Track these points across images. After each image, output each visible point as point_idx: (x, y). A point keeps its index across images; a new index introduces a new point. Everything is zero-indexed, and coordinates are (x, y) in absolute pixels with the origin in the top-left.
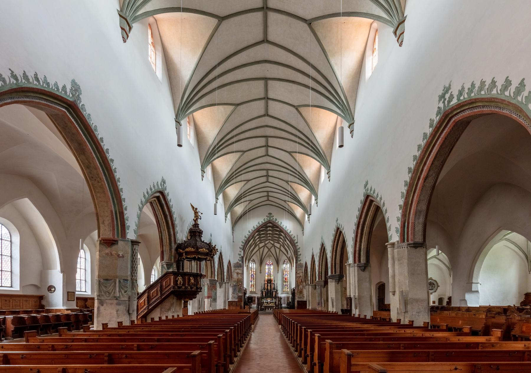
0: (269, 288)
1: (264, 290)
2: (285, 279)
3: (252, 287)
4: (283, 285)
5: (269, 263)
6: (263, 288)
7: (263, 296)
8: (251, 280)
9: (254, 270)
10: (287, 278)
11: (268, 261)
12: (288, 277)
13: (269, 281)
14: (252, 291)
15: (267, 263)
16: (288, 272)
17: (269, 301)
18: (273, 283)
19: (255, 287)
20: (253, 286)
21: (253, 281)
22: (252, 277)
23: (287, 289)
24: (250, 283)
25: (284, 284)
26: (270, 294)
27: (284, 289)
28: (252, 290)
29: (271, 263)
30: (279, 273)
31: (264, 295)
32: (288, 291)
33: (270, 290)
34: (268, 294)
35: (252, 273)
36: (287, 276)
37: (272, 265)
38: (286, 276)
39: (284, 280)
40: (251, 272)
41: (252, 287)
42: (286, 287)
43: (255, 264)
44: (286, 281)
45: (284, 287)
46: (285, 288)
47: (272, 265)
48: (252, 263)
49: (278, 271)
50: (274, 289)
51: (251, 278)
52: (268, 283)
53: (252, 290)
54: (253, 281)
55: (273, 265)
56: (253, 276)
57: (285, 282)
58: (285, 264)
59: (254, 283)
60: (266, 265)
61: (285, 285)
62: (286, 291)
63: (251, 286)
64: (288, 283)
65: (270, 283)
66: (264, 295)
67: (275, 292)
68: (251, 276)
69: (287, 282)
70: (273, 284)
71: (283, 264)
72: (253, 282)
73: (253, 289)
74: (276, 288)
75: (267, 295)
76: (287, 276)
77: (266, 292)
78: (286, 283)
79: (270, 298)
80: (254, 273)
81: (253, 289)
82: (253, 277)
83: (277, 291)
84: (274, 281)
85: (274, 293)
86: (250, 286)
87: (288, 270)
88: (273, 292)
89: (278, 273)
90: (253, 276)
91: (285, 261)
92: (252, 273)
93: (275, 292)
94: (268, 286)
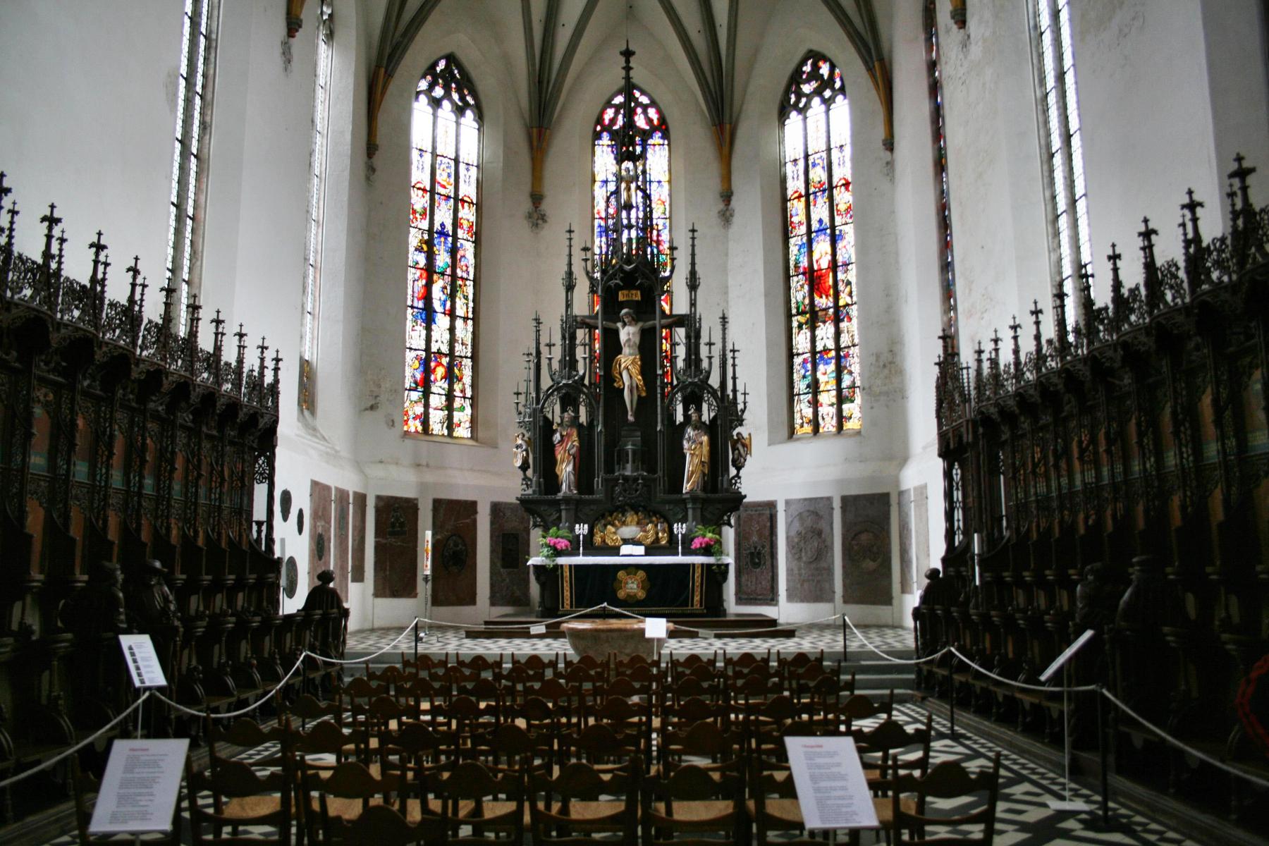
0: (628, 361)
1: (569, 401)
2: (814, 280)
3: (439, 386)
4: (791, 355)
5: (630, 115)
6: (546, 383)
7: (549, 479)
8: (427, 298)
9: (468, 190)
10: (834, 266)
11: (619, 99)
12: (847, 250)
13: (629, 281)
14: (437, 426)
15: (610, 113)
16: (843, 198)
17: (633, 554)
18: (681, 308)
19: (474, 386)
20: (450, 376)
21: (452, 314)
22: (443, 259)
23: (841, 399)
24: (415, 337)
25: (802, 341)
26: (646, 458)
27: (803, 409)
28: (437, 417)
29: (652, 113)
30: (737, 220)
31: (565, 470)
32: (848, 425)
33: (645, 404)
34: (614, 457)
35: (443, 216)
36: (834, 241)
37: (656, 139)
38: (822, 248)
39: (800, 292)
40: (419, 201)
41: (439, 386)
42: (826, 373)
43: (480, 117)
44: (823, 302)
45: (801, 386)
46: (814, 387)
47: (656, 139)
48: (436, 103)
49: (727, 196)
50: (693, 400)
51: (430, 270)
52: (611, 307)
53: (437, 417)
54: (452, 314)
55: (666, 135)
56: (453, 251)
57: (814, 318)
58: (802, 111)
59: (464, 331)
60: (598, 136)
61: (816, 356)
62: (829, 425)
63: (427, 371)
64: (851, 328)
65: (646, 309)
66: (565, 470)
67: (711, 429)
68: (428, 248)
69: (837, 320)
70: (680, 321)
71: (783, 114)
72: (442, 322)
73: (449, 407)
74: (714, 381)
75: (598, 482)
76: (834, 241)
77: (586, 432)
78: (825, 333)
79: (647, 510)
80: (468, 214)
81: (449, 407)
82: (454, 266)
83: (730, 414)
84: (693, 284)
85: (695, 449)
86: (412, 371)
87: (842, 171)
88: (676, 433)
89: (726, 217)
90: (453, 251)
91: (796, 79)
92: (443, 216)
93: (700, 426)
94: (612, 346)
